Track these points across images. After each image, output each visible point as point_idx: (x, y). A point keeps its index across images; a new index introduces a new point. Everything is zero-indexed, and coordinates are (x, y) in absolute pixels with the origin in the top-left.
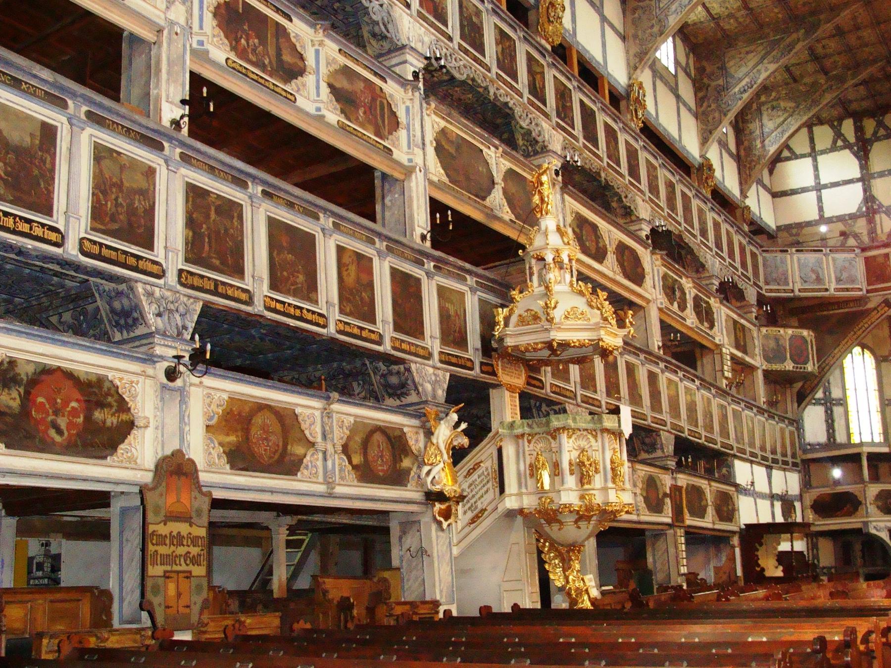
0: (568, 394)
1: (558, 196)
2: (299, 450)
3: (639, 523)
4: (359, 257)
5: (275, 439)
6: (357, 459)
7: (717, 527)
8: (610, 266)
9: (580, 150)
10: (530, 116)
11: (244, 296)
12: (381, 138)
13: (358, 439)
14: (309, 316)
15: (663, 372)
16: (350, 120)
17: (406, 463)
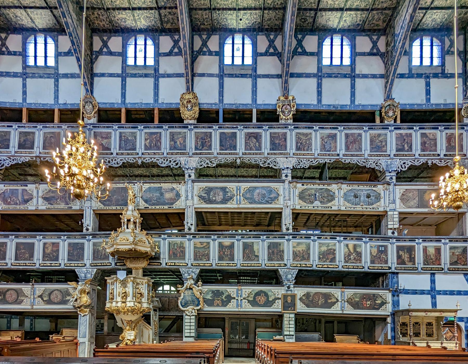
0: (181, 264)
1: (190, 185)
2: (22, 298)
3: (239, 311)
4: (53, 244)
5: (14, 296)
6: (45, 299)
7: (345, 312)
8: (235, 202)
9: (214, 157)
10: (169, 160)
11: (5, 264)
12: (68, 205)
13: (47, 293)
14: (29, 264)
15: (288, 240)
16: (52, 205)
17: (68, 298)
